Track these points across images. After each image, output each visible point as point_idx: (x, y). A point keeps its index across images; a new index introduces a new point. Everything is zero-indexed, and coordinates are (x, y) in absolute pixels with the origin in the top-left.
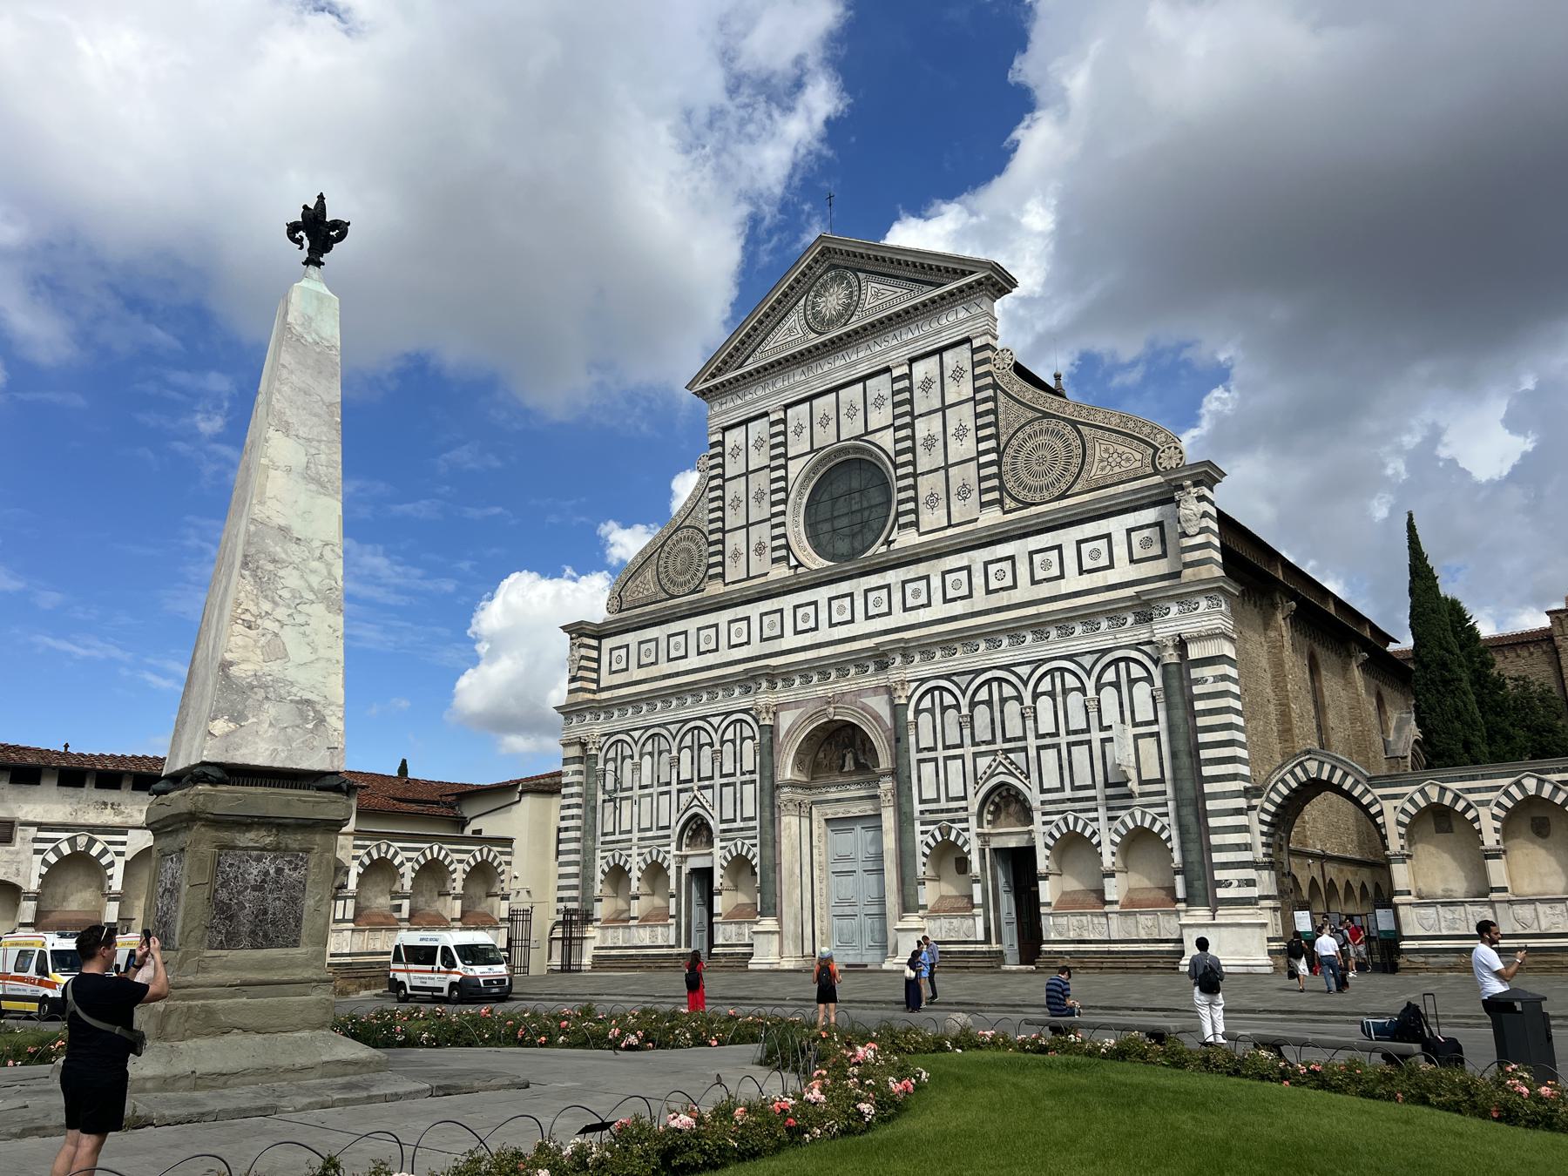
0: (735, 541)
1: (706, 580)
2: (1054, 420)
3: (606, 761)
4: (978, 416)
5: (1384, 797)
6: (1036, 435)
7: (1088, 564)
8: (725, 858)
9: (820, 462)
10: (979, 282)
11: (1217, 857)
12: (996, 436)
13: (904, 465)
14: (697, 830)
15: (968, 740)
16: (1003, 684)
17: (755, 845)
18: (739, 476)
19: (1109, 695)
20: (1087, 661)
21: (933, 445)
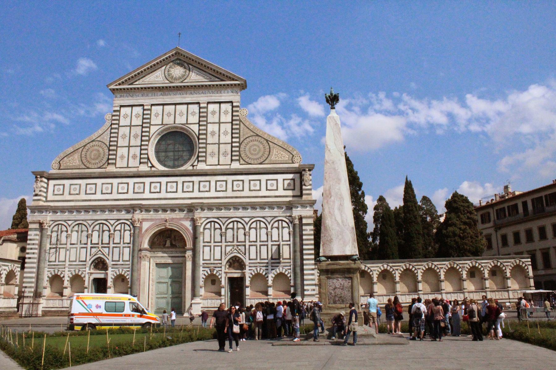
0: (123, 151)
3: (52, 232)
7: (269, 188)
10: (239, 85)
12: (239, 138)
13: (202, 139)
14: (100, 264)
15: (223, 240)
16: (239, 223)
18: (126, 126)
19: (275, 231)
21: (214, 135)
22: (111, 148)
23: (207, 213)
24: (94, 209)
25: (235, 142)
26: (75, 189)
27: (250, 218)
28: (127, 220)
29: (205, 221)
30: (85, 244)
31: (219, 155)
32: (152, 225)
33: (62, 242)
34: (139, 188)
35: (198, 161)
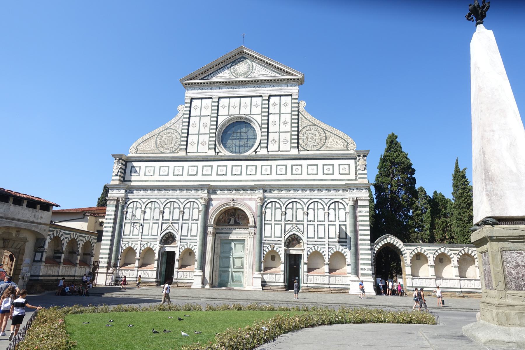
1: (178, 149)
5: (407, 249)
6: (311, 130)
9: (231, 120)
10: (298, 79)
13: (264, 128)
16: (298, 204)
18: (196, 116)
20: (326, 201)
21: (275, 124)
22: (183, 135)
23: (267, 195)
24: (167, 188)
25: (294, 131)
26: (149, 171)
28: (196, 199)
30: (157, 220)
31: (279, 142)
32: (219, 203)
34: (207, 170)
35: (261, 148)
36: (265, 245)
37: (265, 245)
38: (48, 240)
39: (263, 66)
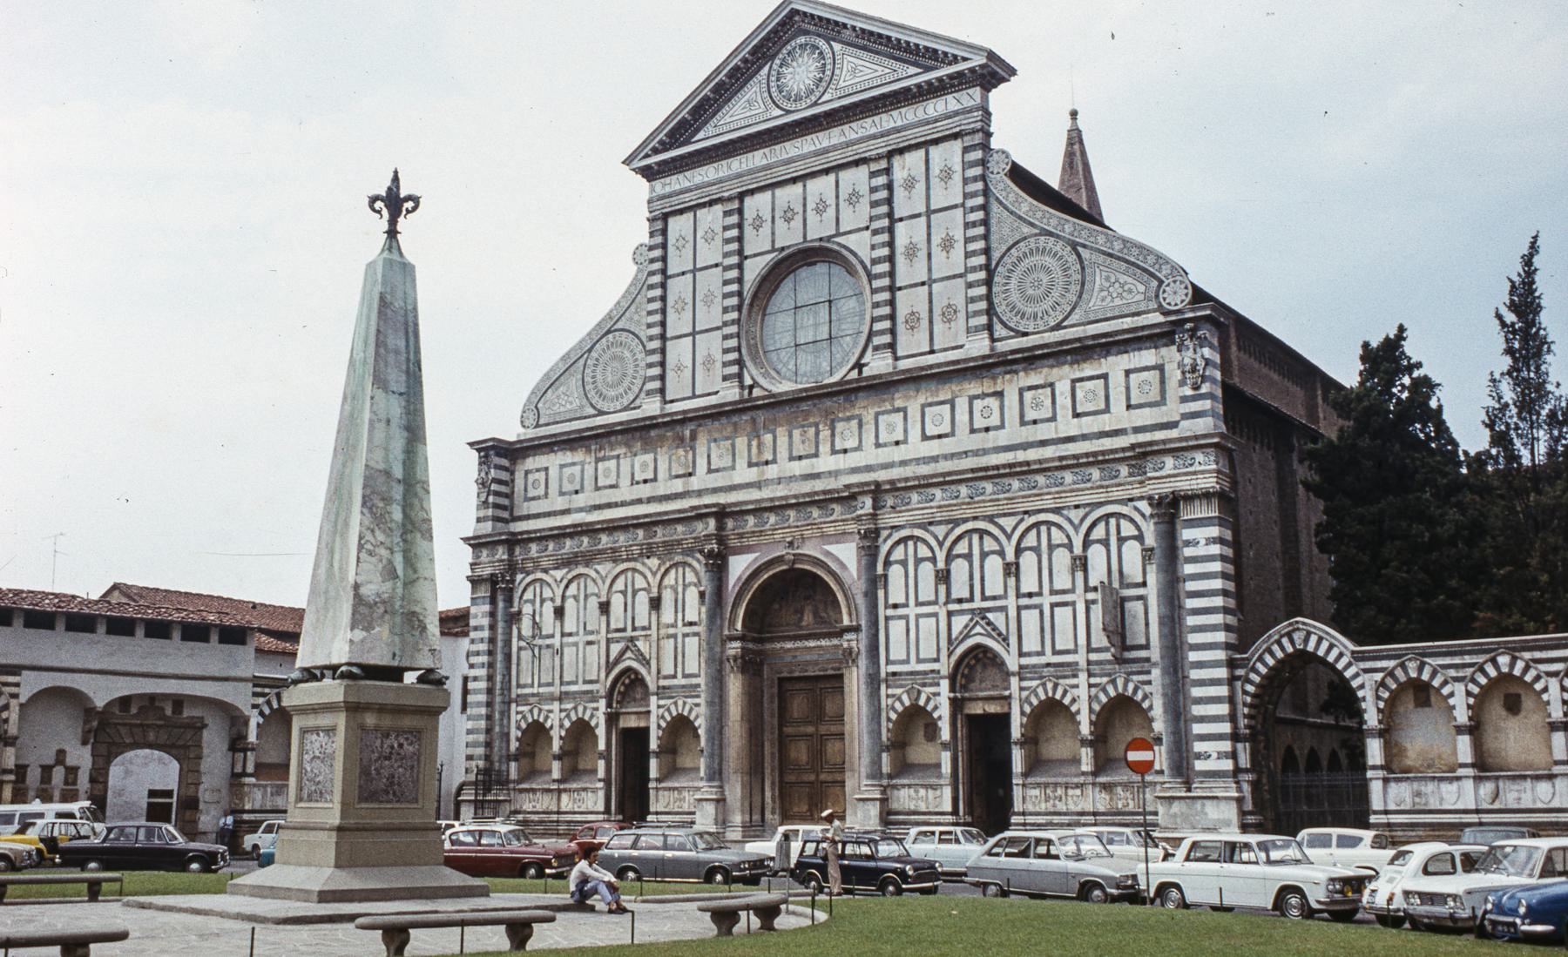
0: (679, 352)
1: (643, 395)
2: (1052, 239)
4: (967, 225)
5: (1366, 671)
8: (663, 717)
10: (972, 70)
11: (1198, 729)
12: (987, 251)
14: (628, 687)
15: (942, 598)
16: (986, 539)
17: (697, 705)
18: (683, 273)
21: (914, 255)
25: (974, 269)
27: (1019, 517)
29: (890, 536)
33: (544, 633)
35: (876, 348)
36: (890, 691)
37: (890, 691)
38: (255, 720)
39: (864, 48)
